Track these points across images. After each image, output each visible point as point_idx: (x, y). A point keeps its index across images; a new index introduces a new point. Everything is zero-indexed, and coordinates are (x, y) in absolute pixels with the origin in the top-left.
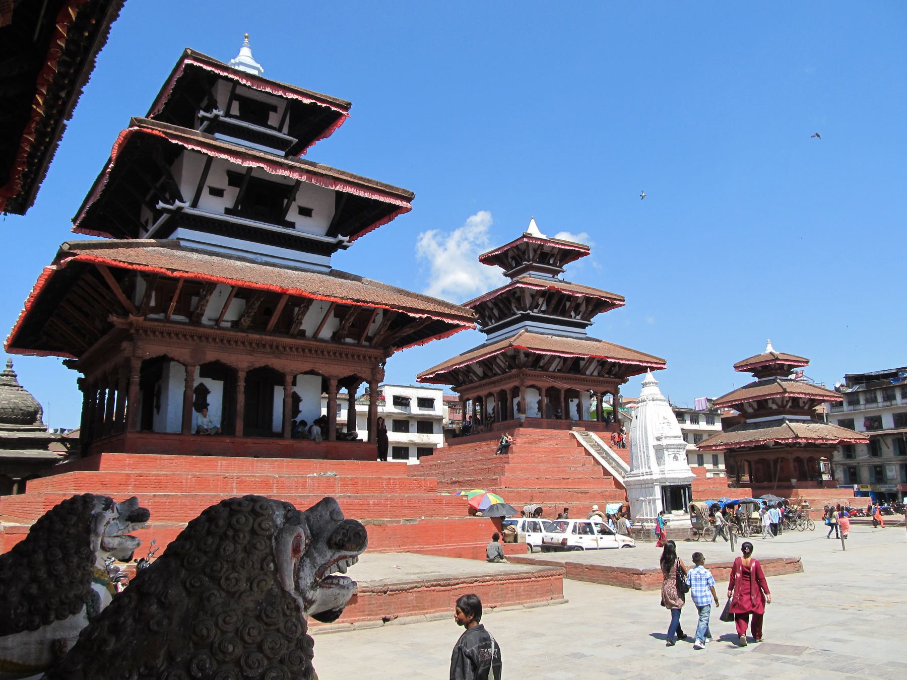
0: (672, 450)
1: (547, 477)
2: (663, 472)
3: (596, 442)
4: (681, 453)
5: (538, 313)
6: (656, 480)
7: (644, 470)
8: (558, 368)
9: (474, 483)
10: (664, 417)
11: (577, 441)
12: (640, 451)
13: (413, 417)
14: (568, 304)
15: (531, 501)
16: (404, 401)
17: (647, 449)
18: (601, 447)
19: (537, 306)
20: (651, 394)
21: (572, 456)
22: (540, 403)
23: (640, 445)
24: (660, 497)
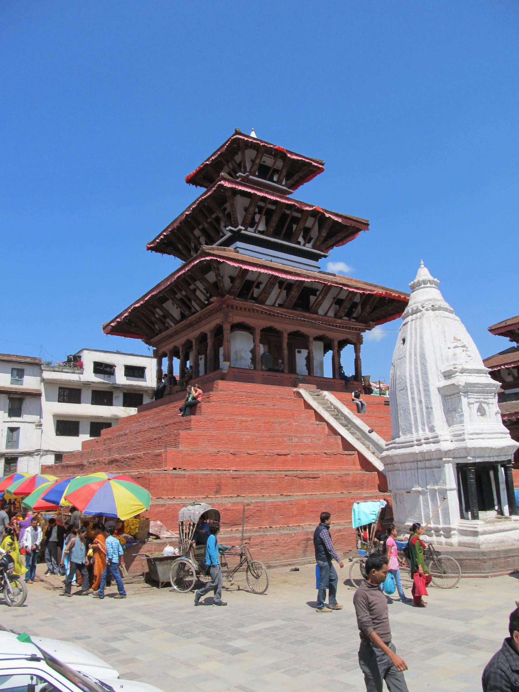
0: (475, 396)
1: (249, 452)
2: (459, 437)
3: (331, 404)
4: (490, 401)
5: (255, 232)
6: (447, 453)
7: (423, 434)
8: (279, 302)
9: (133, 461)
10: (455, 339)
11: (305, 401)
12: (413, 399)
13: (118, 388)
14: (295, 226)
15: (217, 492)
16: (108, 369)
17: (427, 395)
18: (339, 411)
19: (252, 224)
20: (428, 300)
21: (295, 422)
22: (253, 351)
23: (412, 388)
24: (454, 485)
